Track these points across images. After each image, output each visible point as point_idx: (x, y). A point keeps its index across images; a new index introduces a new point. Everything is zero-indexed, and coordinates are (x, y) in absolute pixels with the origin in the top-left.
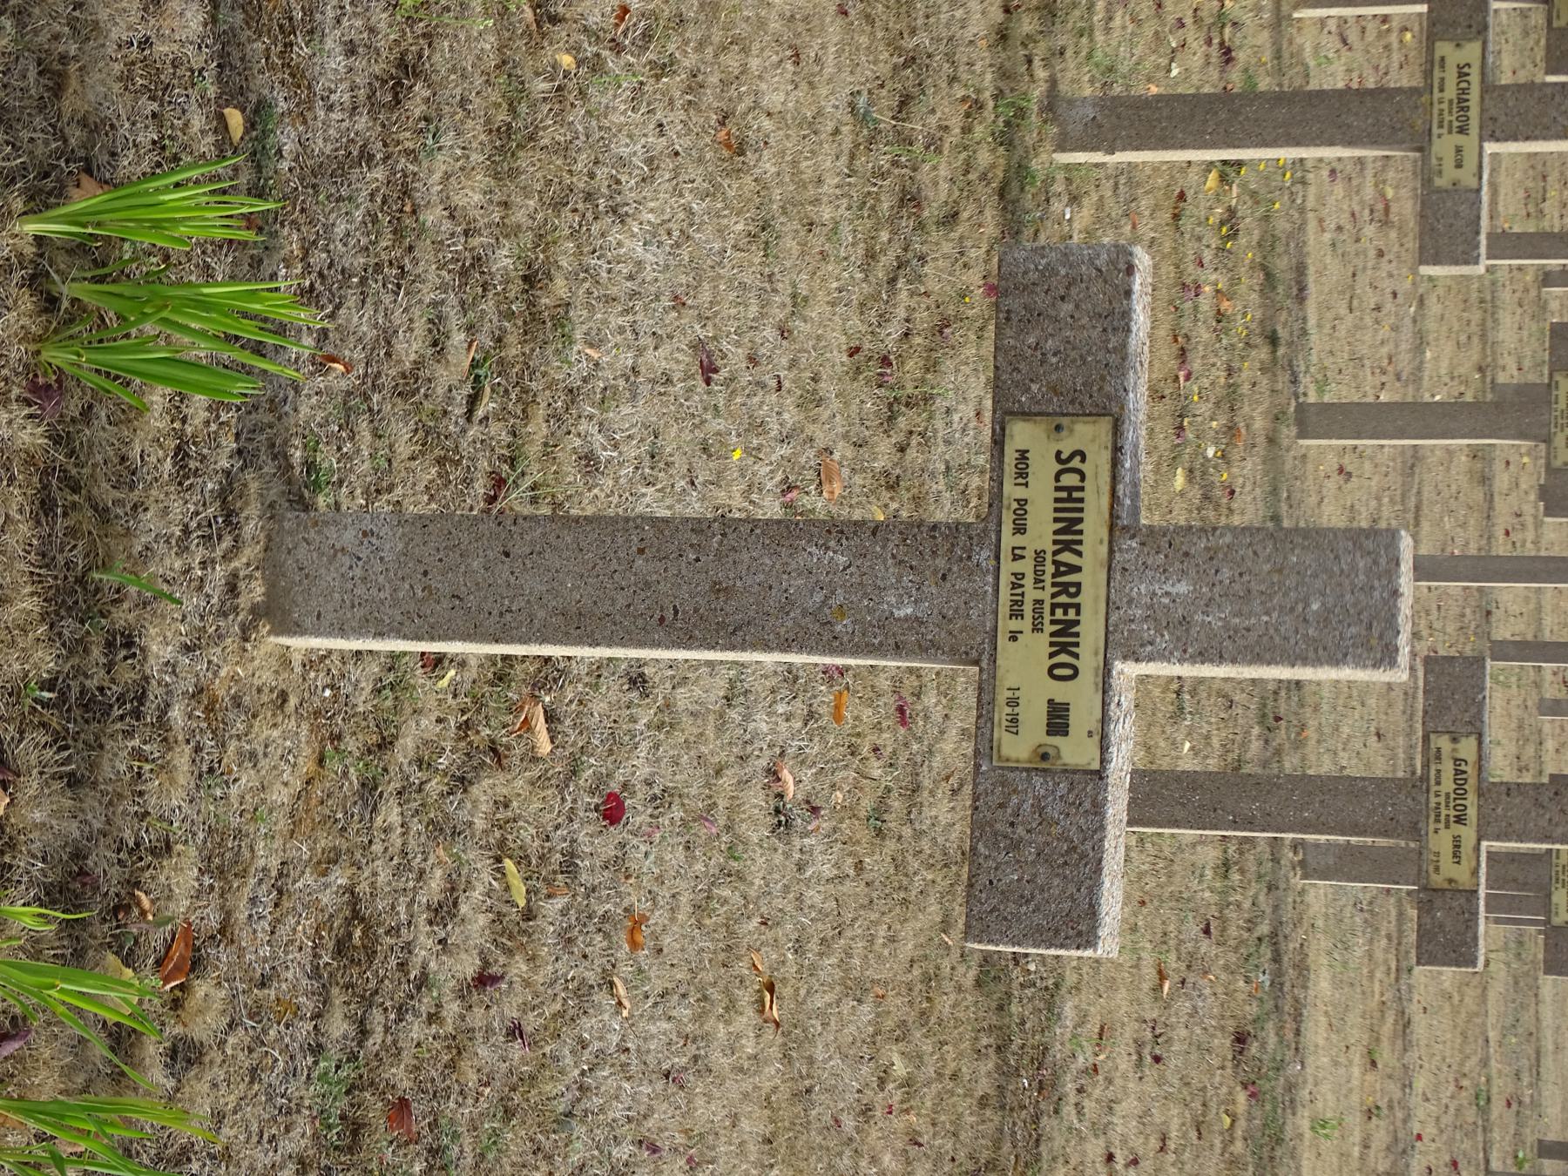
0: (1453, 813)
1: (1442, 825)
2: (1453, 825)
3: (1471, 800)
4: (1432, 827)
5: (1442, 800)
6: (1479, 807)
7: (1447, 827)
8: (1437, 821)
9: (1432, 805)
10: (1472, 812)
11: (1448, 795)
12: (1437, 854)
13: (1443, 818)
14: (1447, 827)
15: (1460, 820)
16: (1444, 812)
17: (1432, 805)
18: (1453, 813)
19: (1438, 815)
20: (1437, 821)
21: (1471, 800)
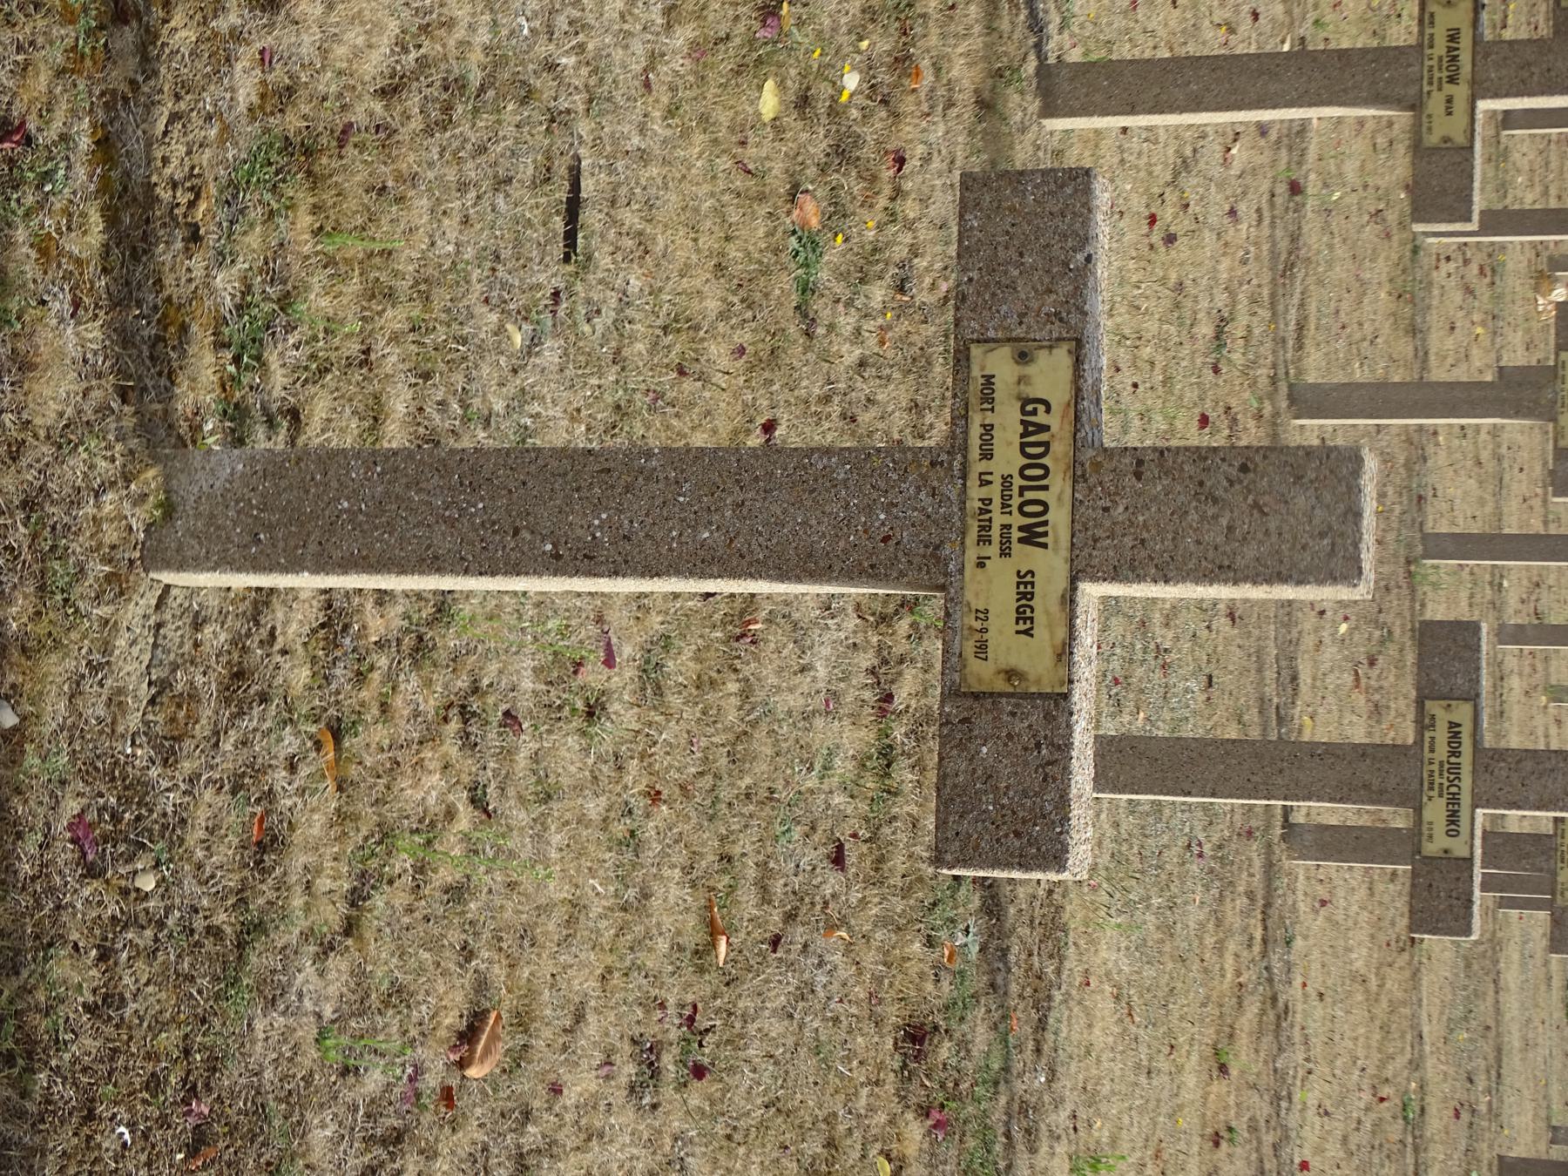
0: (1017, 520)
1: (993, 550)
2: (1016, 547)
3: (1058, 490)
4: (972, 554)
5: (995, 491)
6: (1075, 504)
7: (1005, 552)
8: (984, 540)
9: (974, 505)
10: (1059, 518)
11: (1006, 480)
12: (982, 615)
13: (995, 532)
14: (1005, 552)
15: (1032, 536)
16: (998, 519)
17: (974, 505)
18: (1017, 520)
19: (985, 527)
20: (984, 540)
21: (1058, 490)
